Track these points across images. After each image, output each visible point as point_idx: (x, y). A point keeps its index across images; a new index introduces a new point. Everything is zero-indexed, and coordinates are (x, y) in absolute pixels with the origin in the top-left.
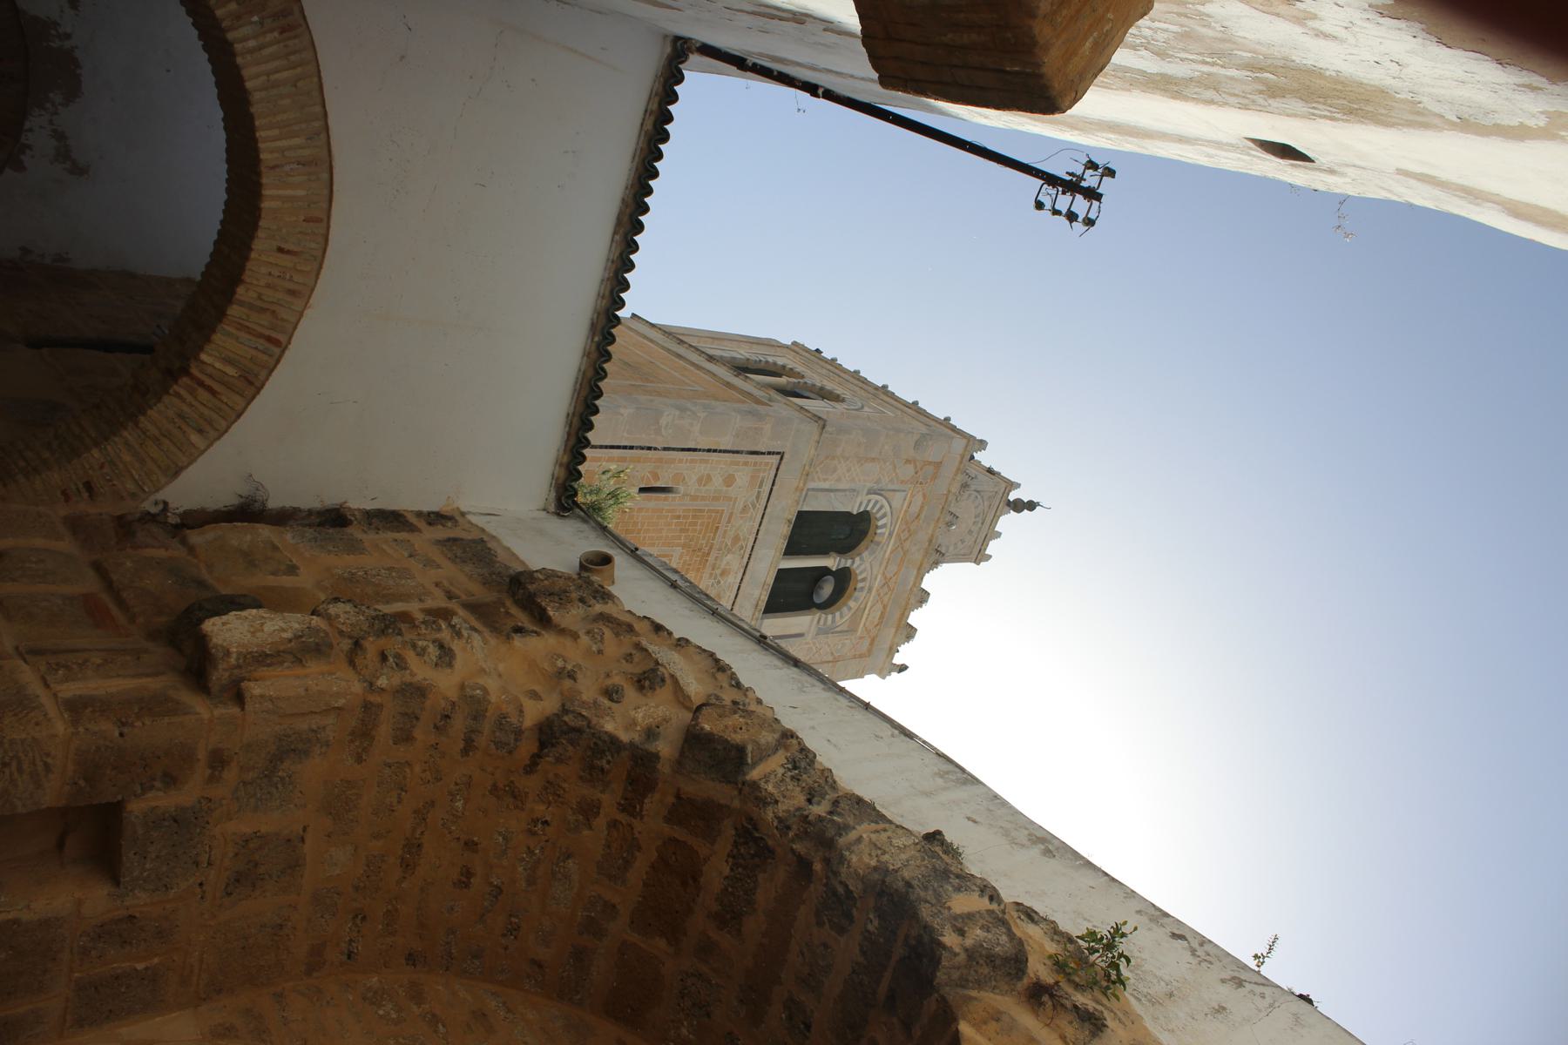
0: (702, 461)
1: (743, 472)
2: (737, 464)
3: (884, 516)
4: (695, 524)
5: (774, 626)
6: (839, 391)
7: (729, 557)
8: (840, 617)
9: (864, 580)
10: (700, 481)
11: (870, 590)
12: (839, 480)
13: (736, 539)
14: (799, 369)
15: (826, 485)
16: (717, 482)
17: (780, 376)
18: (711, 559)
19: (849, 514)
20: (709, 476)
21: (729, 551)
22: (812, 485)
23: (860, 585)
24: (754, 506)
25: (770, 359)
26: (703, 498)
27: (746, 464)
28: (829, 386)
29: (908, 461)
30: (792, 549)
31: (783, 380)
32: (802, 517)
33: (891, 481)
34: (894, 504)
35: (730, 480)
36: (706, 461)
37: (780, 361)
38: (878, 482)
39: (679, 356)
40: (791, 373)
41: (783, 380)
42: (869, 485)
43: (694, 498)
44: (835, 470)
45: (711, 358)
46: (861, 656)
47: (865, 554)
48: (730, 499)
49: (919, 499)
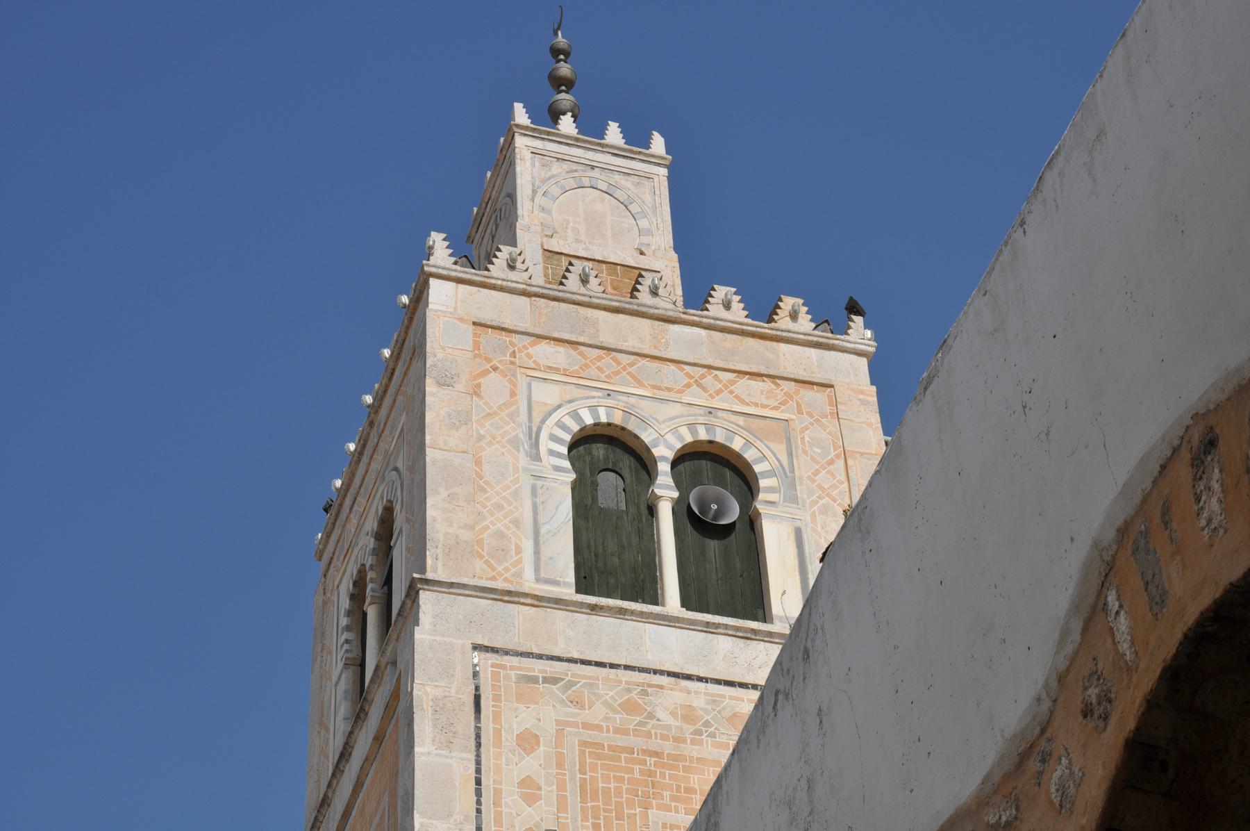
0: (497, 803)
1: (512, 717)
2: (498, 733)
3: (575, 415)
4: (606, 792)
5: (786, 596)
6: (377, 507)
7: (660, 714)
8: (762, 459)
9: (692, 427)
10: (530, 799)
11: (711, 411)
12: (517, 523)
13: (629, 707)
14: (352, 570)
15: (528, 546)
16: (532, 765)
17: (365, 615)
18: (668, 747)
19: (576, 486)
20: (521, 784)
21: (651, 716)
22: (529, 574)
23: (703, 435)
24: (571, 684)
25: (344, 621)
26: (561, 786)
27: (497, 717)
28: (371, 524)
29: (476, 392)
30: (644, 587)
31: (372, 613)
32: (584, 583)
33: (513, 416)
34: (553, 400)
35: (528, 741)
36: (498, 793)
37: (345, 603)
38: (515, 443)
39: (346, 815)
40: (360, 582)
41: (372, 613)
42: (523, 460)
43: (562, 804)
44: (500, 535)
45: (345, 754)
46: (835, 403)
47: (647, 437)
48: (560, 732)
49: (545, 353)
